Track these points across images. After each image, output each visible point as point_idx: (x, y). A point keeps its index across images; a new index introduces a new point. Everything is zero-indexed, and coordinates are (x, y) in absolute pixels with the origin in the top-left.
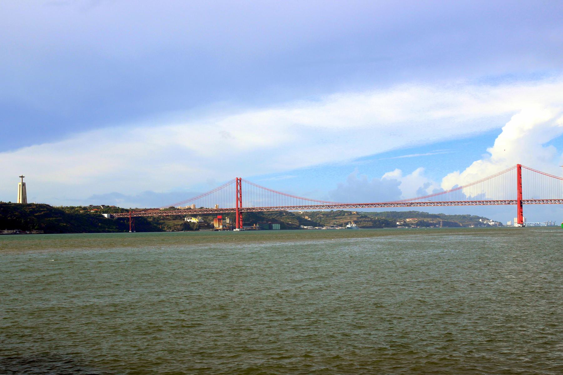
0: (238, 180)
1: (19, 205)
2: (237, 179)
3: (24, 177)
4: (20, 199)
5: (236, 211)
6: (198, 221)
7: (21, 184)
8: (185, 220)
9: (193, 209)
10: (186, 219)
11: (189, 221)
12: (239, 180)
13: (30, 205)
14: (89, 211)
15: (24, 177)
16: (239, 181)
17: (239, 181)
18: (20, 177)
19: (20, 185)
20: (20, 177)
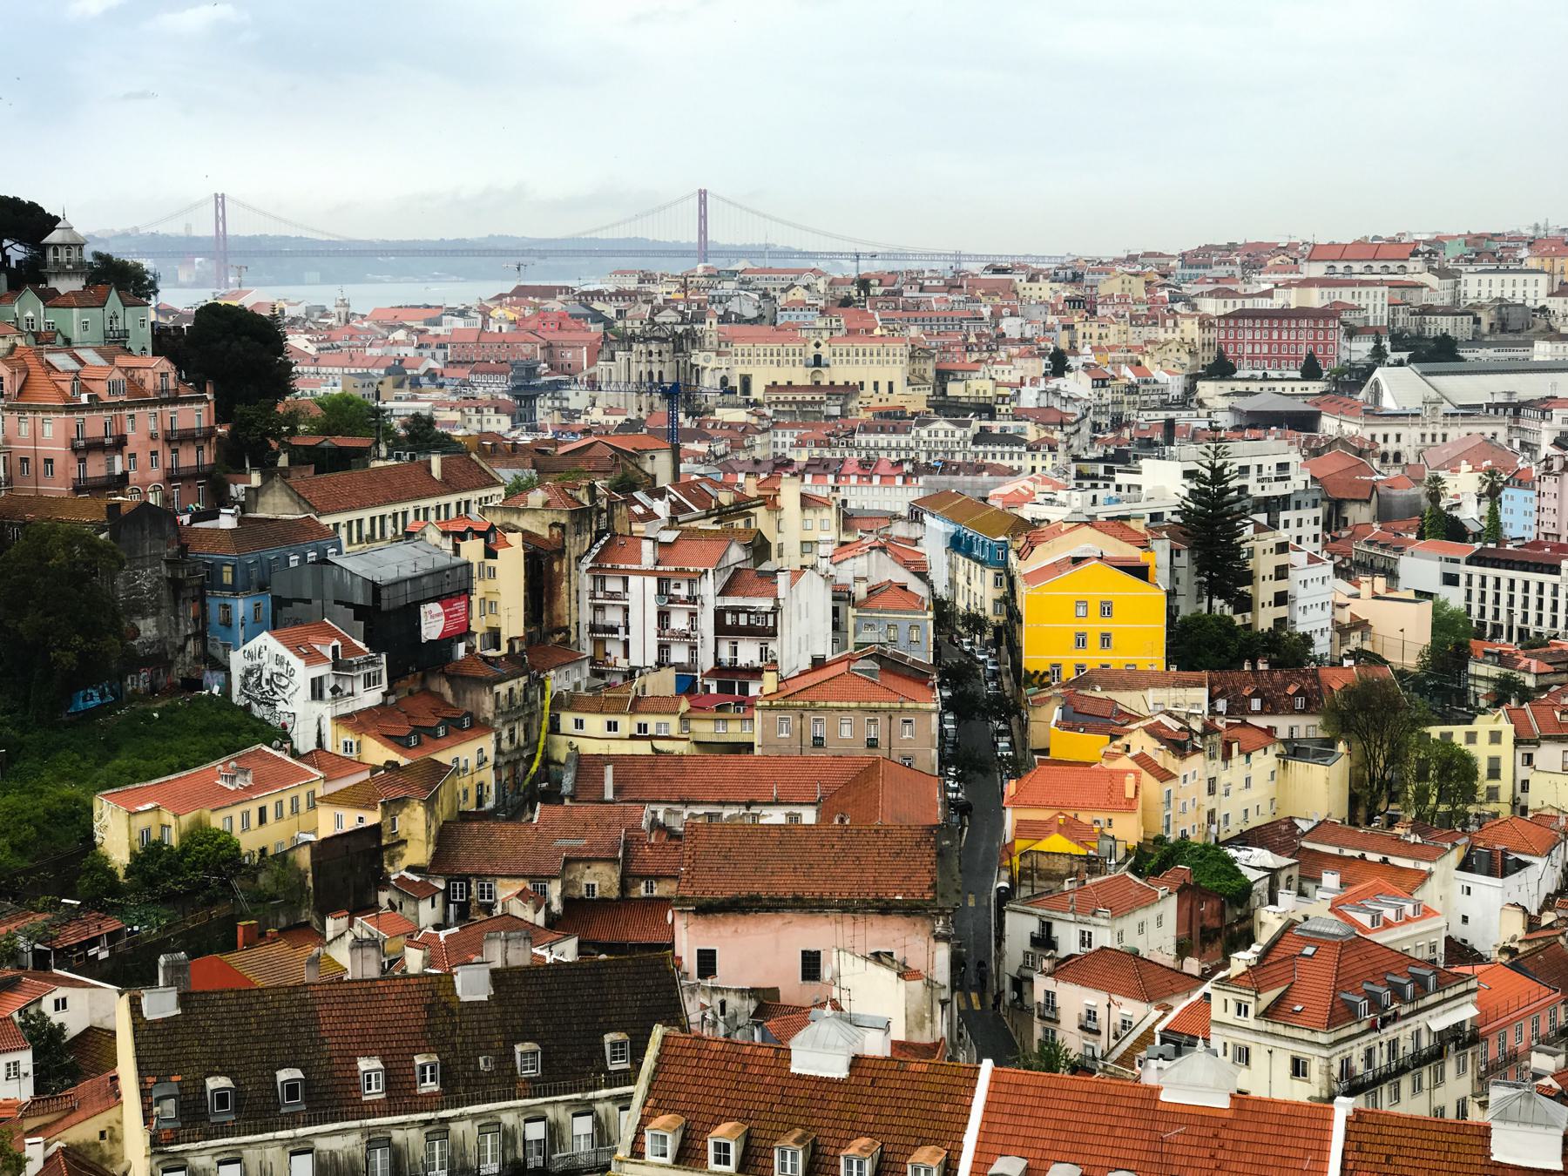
2: (216, 196)
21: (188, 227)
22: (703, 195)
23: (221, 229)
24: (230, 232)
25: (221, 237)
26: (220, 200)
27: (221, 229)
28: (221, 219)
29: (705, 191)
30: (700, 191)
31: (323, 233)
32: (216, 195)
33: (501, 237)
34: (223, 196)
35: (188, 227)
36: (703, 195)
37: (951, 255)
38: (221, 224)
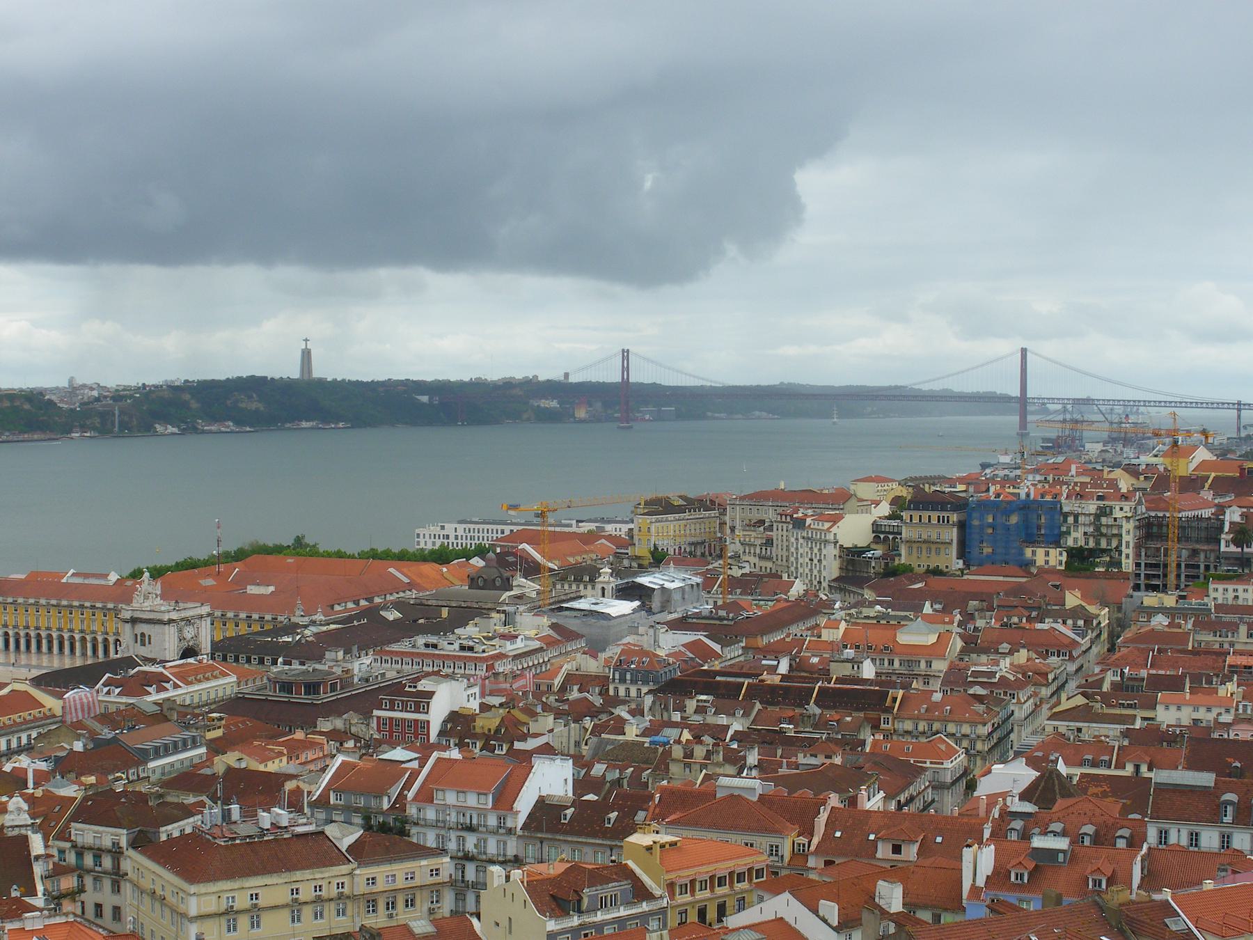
2: (623, 350)
13: (321, 382)
16: (626, 354)
17: (626, 354)
21: (567, 375)
22: (1024, 352)
23: (625, 377)
24: (630, 381)
25: (625, 383)
26: (625, 354)
27: (625, 377)
28: (626, 369)
29: (1026, 349)
30: (1022, 348)
31: (707, 380)
33: (790, 384)
34: (628, 350)
35: (567, 375)
36: (1024, 352)
37: (1234, 404)
38: (625, 373)
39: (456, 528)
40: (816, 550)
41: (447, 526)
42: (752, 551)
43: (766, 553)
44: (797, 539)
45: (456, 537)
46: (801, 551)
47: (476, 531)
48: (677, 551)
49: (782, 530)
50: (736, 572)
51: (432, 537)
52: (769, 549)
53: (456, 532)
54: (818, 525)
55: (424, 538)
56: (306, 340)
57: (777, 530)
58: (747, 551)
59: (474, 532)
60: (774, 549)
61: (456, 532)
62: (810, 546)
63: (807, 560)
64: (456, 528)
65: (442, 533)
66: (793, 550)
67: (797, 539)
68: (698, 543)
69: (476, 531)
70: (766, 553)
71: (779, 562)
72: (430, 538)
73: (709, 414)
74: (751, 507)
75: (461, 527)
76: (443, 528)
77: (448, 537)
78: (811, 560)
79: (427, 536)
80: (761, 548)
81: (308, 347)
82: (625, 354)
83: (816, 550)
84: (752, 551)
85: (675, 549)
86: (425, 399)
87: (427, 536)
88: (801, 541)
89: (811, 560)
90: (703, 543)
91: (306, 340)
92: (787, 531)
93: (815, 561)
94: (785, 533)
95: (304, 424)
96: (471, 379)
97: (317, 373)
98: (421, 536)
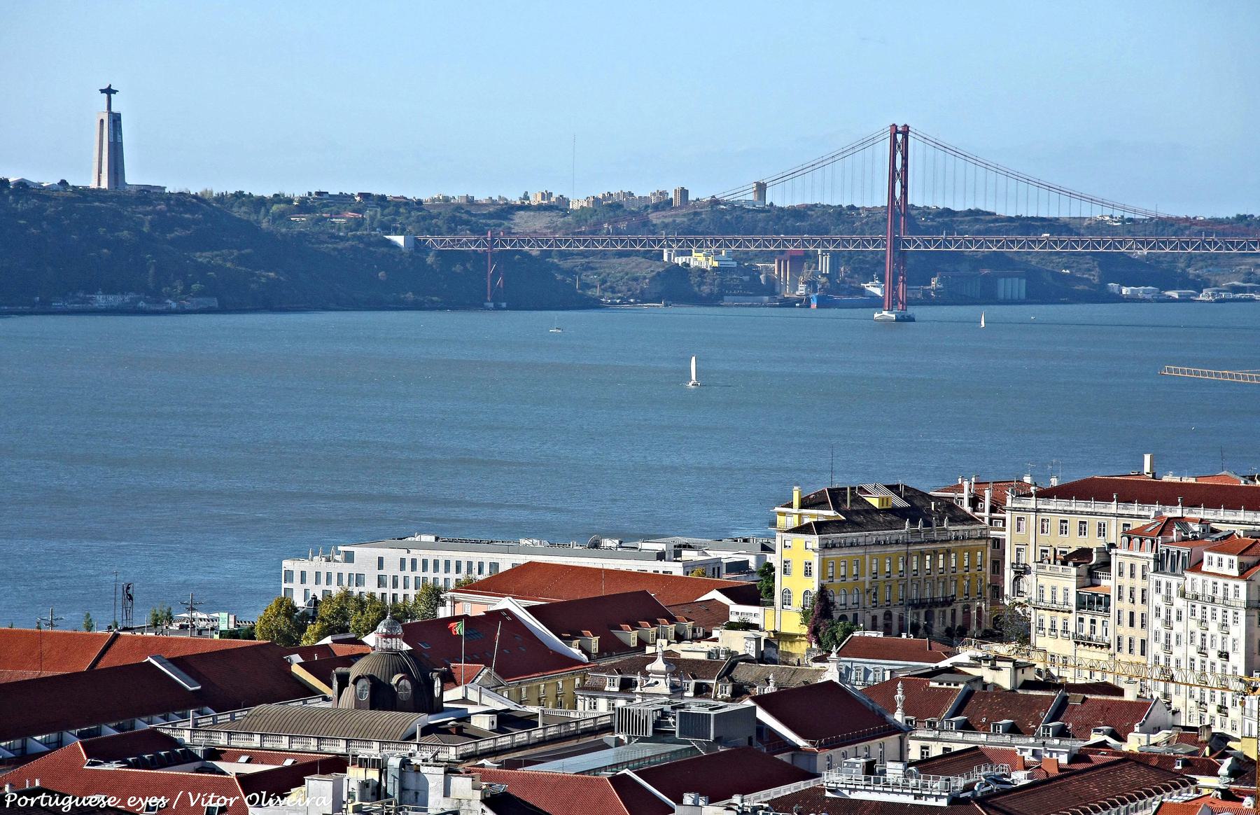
0: (897, 132)
1: (96, 194)
2: (895, 130)
3: (115, 92)
4: (100, 172)
5: (885, 246)
6: (716, 264)
7: (106, 117)
8: (665, 258)
9: (680, 207)
10: (669, 255)
11: (680, 260)
12: (900, 133)
13: (148, 195)
14: (326, 218)
15: (115, 92)
16: (899, 137)
17: (899, 137)
18: (102, 91)
19: (102, 121)
20: (102, 91)
21: (761, 188)
25: (900, 211)
26: (900, 138)
28: (899, 175)
32: (894, 126)
34: (906, 132)
35: (761, 188)
38: (898, 185)
39: (381, 560)
40: (1213, 627)
41: (358, 551)
42: (1059, 627)
43: (1093, 630)
44: (1168, 598)
45: (381, 582)
46: (1178, 627)
47: (431, 565)
48: (880, 621)
49: (1132, 575)
50: (1003, 678)
51: (323, 578)
52: (1099, 620)
53: (380, 566)
54: (1220, 565)
55: (303, 581)
56: (109, 91)
57: (1121, 574)
58: (1047, 625)
59: (425, 568)
60: (1112, 621)
61: (380, 566)
62: (1199, 615)
63: (1193, 651)
64: (381, 560)
65: (346, 569)
66: (1156, 624)
67: (1168, 598)
68: (934, 603)
69: (431, 565)
70: (1093, 630)
71: (1124, 656)
72: (317, 582)
73: (1113, 286)
74: (1064, 517)
75: (392, 555)
76: (349, 557)
77: (360, 579)
78: (1202, 651)
79: (310, 578)
80: (1081, 620)
81: (113, 110)
82: (900, 138)
83: (1213, 627)
84: (1059, 627)
85: (874, 618)
86: (399, 240)
87: (310, 578)
88: (1179, 603)
89: (1202, 651)
90: (948, 602)
91: (109, 91)
92: (1144, 577)
93: (1213, 655)
94: (1139, 583)
95: (100, 300)
96: (526, 197)
97: (134, 177)
98: (297, 577)
